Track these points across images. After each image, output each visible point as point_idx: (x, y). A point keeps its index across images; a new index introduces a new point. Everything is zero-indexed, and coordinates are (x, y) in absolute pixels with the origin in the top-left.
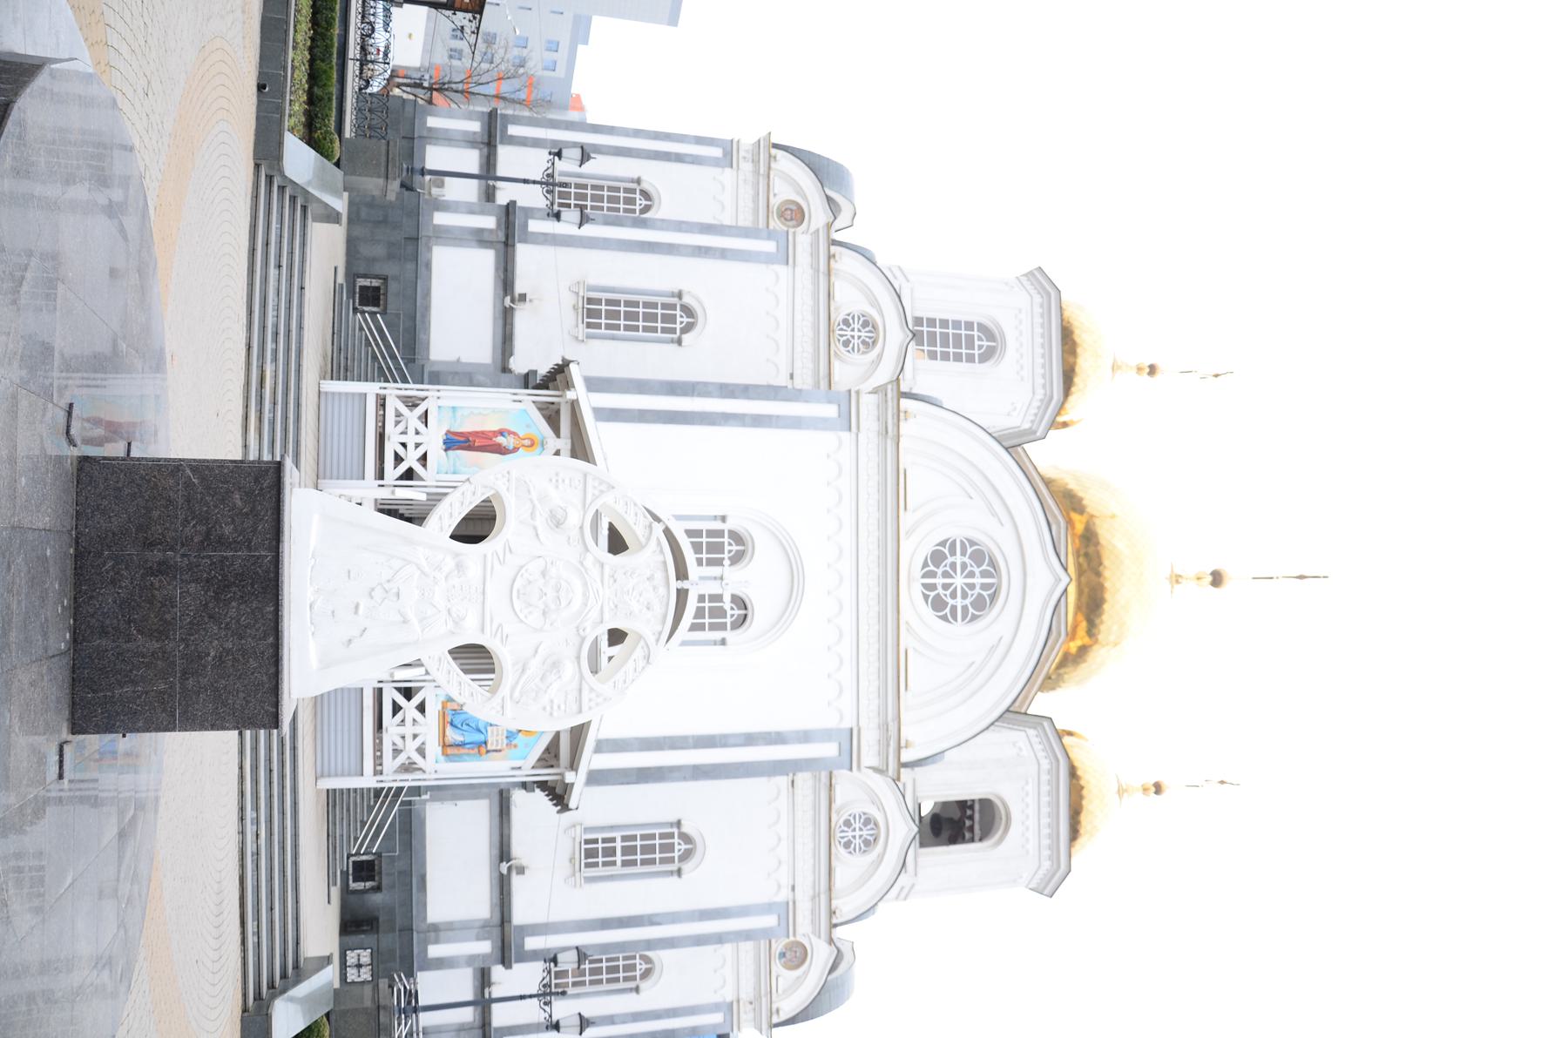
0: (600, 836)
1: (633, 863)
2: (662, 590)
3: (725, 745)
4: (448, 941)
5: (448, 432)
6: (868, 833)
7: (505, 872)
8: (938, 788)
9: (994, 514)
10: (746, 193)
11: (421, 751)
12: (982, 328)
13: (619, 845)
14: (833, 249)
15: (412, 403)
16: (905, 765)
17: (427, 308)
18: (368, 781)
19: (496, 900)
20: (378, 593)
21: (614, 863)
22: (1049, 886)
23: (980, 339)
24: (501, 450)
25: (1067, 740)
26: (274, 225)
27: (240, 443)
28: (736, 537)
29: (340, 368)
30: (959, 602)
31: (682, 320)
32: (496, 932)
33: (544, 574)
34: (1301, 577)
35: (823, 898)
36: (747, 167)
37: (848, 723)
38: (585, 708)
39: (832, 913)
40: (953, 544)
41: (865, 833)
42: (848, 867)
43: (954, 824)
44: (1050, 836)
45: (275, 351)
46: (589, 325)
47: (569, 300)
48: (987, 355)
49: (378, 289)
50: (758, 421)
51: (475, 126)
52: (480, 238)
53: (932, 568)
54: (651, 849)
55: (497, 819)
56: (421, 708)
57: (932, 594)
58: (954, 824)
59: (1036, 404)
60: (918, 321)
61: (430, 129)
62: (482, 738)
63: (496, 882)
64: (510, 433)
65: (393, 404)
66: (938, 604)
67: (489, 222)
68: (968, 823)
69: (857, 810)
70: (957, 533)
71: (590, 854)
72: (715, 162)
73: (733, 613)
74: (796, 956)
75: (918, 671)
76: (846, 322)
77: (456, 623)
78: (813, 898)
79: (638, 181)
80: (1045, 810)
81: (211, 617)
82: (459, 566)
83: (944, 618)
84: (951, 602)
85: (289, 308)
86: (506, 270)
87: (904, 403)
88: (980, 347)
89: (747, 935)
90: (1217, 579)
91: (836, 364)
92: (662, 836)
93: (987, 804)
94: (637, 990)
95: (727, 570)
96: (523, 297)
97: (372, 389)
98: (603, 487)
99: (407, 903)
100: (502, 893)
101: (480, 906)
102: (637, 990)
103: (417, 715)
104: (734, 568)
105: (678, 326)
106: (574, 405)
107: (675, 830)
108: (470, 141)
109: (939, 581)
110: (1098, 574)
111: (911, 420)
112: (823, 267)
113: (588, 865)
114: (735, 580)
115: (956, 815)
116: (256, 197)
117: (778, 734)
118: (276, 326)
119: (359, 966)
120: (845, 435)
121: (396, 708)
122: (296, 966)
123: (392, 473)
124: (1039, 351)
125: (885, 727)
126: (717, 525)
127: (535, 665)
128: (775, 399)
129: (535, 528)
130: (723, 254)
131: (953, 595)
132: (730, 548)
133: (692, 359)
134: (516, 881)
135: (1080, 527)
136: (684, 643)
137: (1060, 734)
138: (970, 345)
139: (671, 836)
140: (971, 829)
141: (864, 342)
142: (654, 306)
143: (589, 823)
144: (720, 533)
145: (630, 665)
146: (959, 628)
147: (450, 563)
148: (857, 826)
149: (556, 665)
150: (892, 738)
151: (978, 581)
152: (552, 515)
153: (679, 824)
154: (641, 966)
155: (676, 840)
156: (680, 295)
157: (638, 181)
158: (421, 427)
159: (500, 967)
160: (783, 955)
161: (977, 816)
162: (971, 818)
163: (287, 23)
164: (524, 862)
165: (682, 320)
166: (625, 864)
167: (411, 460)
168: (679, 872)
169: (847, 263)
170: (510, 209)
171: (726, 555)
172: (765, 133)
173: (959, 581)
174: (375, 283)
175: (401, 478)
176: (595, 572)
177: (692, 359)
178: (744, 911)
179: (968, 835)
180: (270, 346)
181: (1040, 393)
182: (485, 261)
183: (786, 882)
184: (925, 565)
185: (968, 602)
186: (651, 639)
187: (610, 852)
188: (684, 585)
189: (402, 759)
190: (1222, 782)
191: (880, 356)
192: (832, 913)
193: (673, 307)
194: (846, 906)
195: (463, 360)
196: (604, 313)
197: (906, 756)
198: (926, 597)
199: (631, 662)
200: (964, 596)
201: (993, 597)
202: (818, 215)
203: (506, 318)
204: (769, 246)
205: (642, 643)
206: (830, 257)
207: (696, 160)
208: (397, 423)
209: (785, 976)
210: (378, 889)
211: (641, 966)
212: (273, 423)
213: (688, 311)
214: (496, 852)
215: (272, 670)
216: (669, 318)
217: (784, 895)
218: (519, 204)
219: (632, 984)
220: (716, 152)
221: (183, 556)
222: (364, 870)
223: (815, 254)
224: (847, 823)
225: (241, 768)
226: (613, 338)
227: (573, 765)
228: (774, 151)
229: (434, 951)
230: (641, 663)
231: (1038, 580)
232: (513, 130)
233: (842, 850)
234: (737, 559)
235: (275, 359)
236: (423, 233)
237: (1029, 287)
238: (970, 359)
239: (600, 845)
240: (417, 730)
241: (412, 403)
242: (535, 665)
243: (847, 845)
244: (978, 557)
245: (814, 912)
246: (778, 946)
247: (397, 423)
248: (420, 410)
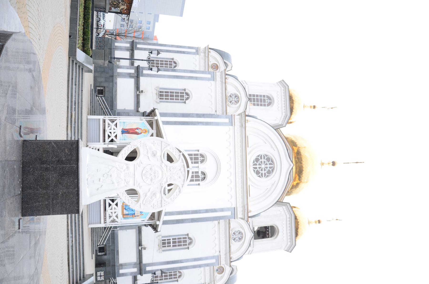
0: (166, 239)
1: (176, 246)
2: (183, 173)
3: (200, 213)
4: (125, 268)
5: (123, 129)
6: (240, 236)
7: (140, 249)
8: (259, 223)
9: (272, 147)
10: (202, 61)
11: (117, 217)
12: (267, 97)
13: (171, 241)
14: (227, 76)
15: (112, 121)
16: (250, 217)
17: (116, 95)
18: (102, 225)
19: (138, 257)
20: (106, 175)
21: (170, 246)
22: (290, 249)
23: (267, 100)
24: (137, 133)
25: (294, 209)
26: (74, 74)
27: (66, 133)
28: (202, 156)
29: (93, 112)
30: (263, 172)
31: (186, 96)
32: (138, 266)
33: (151, 169)
34: (357, 163)
35: (228, 254)
36: (202, 54)
37: (234, 206)
38: (163, 206)
39: (230, 258)
40: (261, 156)
41: (239, 236)
42: (235, 245)
43: (263, 233)
44: (290, 236)
45: (75, 108)
46: (160, 99)
47: (155, 92)
48: (269, 104)
49: (102, 90)
50: (207, 124)
51: (128, 45)
52: (130, 76)
53: (256, 163)
54: (180, 242)
55: (138, 235)
56: (117, 205)
57: (256, 170)
58: (263, 233)
59: (283, 117)
60: (250, 95)
61: (116, 46)
62: (133, 212)
63: (138, 252)
64: (140, 129)
65: (107, 122)
66: (258, 173)
67: (132, 71)
68: (267, 233)
69: (237, 230)
70: (262, 153)
71: (164, 243)
72: (194, 53)
73: (201, 176)
74: (221, 270)
75: (253, 192)
76: (230, 96)
77: (127, 183)
78: (225, 254)
79: (173, 59)
80: (288, 228)
81: (60, 183)
82: (128, 168)
83: (259, 176)
84: (261, 172)
85: (79, 96)
86: (137, 84)
87: (247, 118)
88: (267, 102)
89: (207, 265)
90: (334, 164)
91: (228, 108)
92: (183, 238)
93: (272, 227)
94: (177, 281)
95: (200, 164)
96: (142, 91)
97: (101, 117)
98: (167, 145)
99: (114, 258)
100: (140, 255)
101: (134, 259)
102: (177, 281)
103: (116, 207)
104: (202, 164)
105: (185, 98)
106: (157, 121)
107: (187, 237)
108: (127, 49)
109: (258, 166)
110: (301, 163)
111: (249, 122)
112: (224, 81)
113: (163, 247)
114: (202, 167)
115: (264, 230)
116: (69, 66)
117: (215, 209)
118: (75, 101)
119: (101, 276)
120: (231, 127)
121: (110, 205)
122: (84, 277)
123: (107, 140)
124: (283, 103)
125: (244, 207)
126: (197, 152)
127: (149, 194)
128: (212, 118)
129: (148, 157)
130: (196, 78)
131: (262, 170)
132: (200, 159)
133: (188, 107)
134: (144, 252)
135: (296, 151)
136: (189, 185)
137: (292, 208)
138: (264, 101)
139: (186, 238)
140: (268, 234)
141: (235, 101)
142: (178, 93)
143: (163, 235)
144: (197, 155)
145: (175, 193)
146: (263, 179)
147: (125, 167)
148: (237, 234)
149: (155, 194)
150: (246, 209)
151: (268, 166)
152: (153, 153)
153: (188, 235)
154: (178, 274)
155: (187, 239)
156: (185, 90)
157: (173, 59)
158: (115, 128)
159: (140, 275)
160: (217, 270)
161: (270, 231)
162: (268, 231)
163: (77, 19)
164: (146, 246)
166: (173, 246)
167: (113, 137)
168: (188, 248)
169: (230, 80)
170: (138, 67)
171: (199, 161)
172: (207, 45)
173: (263, 166)
174: (102, 88)
175: (110, 142)
176: (165, 168)
177: (188, 107)
178: (206, 258)
179: (267, 236)
180: (73, 107)
181: (284, 114)
182: (132, 81)
183: (218, 250)
184: (254, 162)
185: (266, 172)
186: (181, 186)
187: (169, 243)
188: (189, 169)
189: (112, 219)
190: (337, 220)
191: (240, 105)
192: (230, 258)
193: (183, 93)
194: (234, 256)
195: (126, 109)
196: (164, 95)
197: (250, 215)
198: (254, 171)
199: (175, 192)
200: (265, 170)
201: (273, 170)
202: (222, 67)
203: (137, 97)
204: (209, 76)
205: (178, 188)
206: (226, 78)
207: (188, 53)
208: (109, 127)
209: (218, 276)
210: (106, 254)
211: (178, 274)
212: (75, 127)
213: (187, 94)
214: (138, 244)
215: (77, 198)
216: (182, 96)
217: (217, 254)
218: (141, 66)
219: (176, 279)
220: (194, 51)
221: (52, 167)
222: (102, 249)
223: (221, 78)
224: (234, 233)
225: (68, 222)
226: (167, 102)
227: (159, 219)
228: (209, 50)
229: (121, 271)
230: (178, 193)
231: (285, 165)
232: (138, 46)
233: (233, 241)
234: (202, 161)
235: (75, 110)
236: (114, 74)
237: (280, 85)
238: (265, 105)
239: (166, 241)
240: (116, 211)
241: (112, 121)
242: (149, 194)
243: (234, 239)
244: (268, 159)
245: (226, 258)
246: (216, 268)
247: (109, 127)
248: (115, 123)
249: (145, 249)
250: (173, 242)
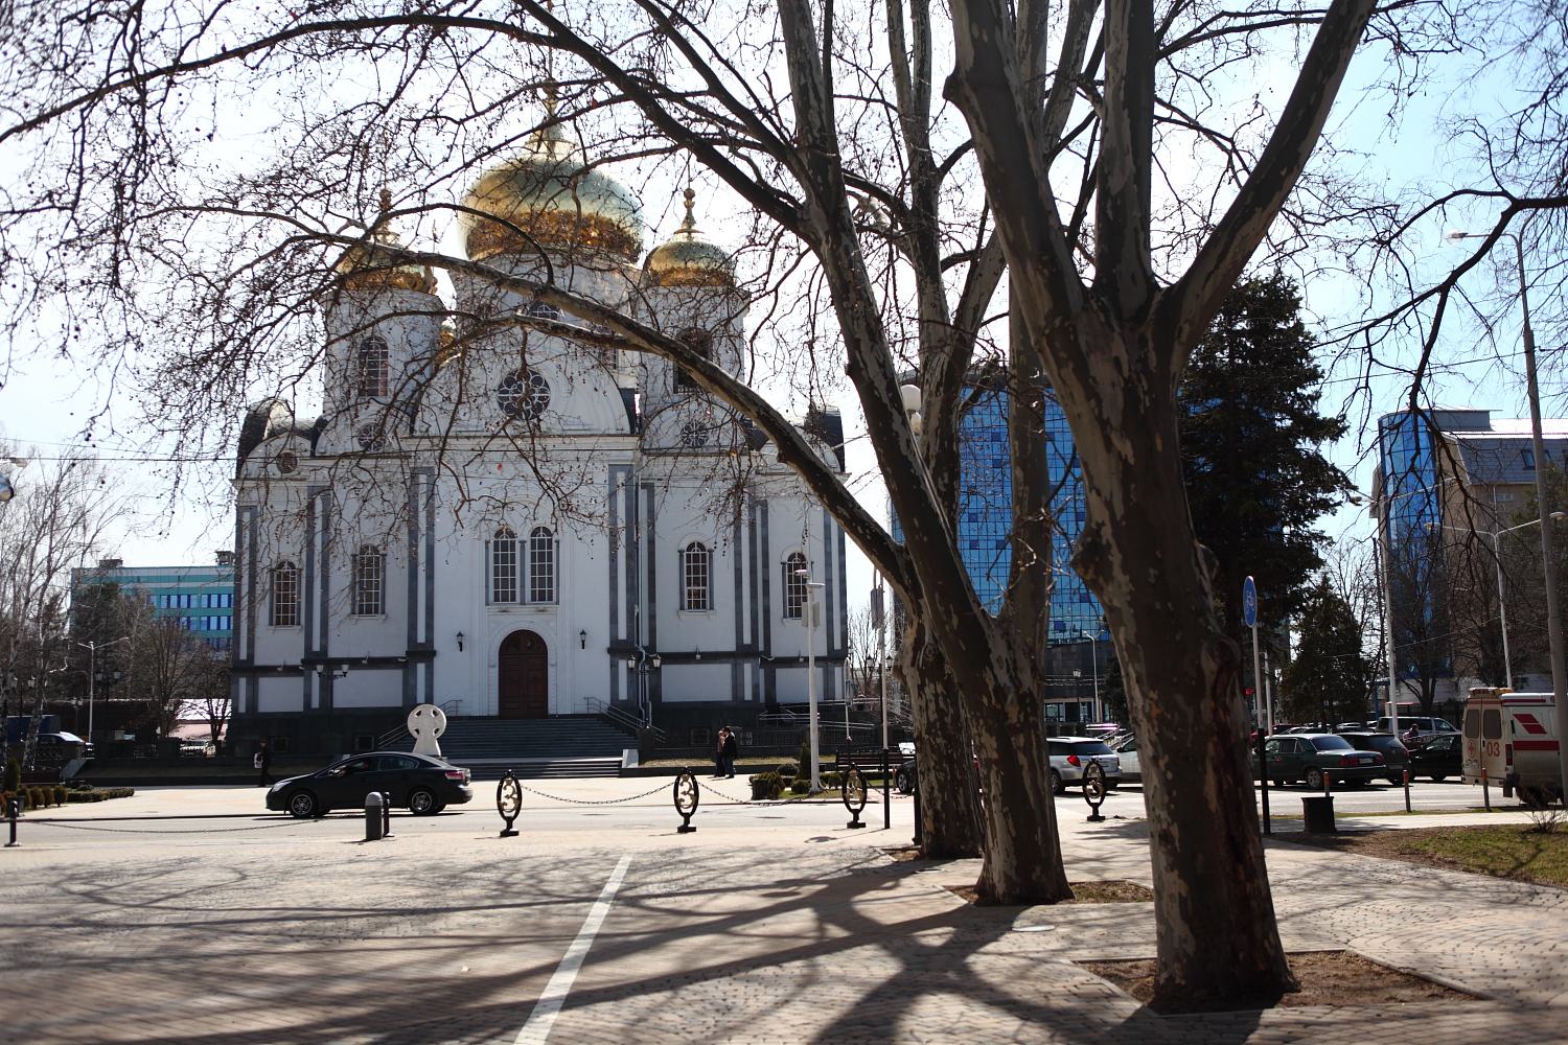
1: (704, 579)
114: (524, 533)
146: (553, 395)
187: (697, 594)
196: (368, 601)
232: (243, 656)
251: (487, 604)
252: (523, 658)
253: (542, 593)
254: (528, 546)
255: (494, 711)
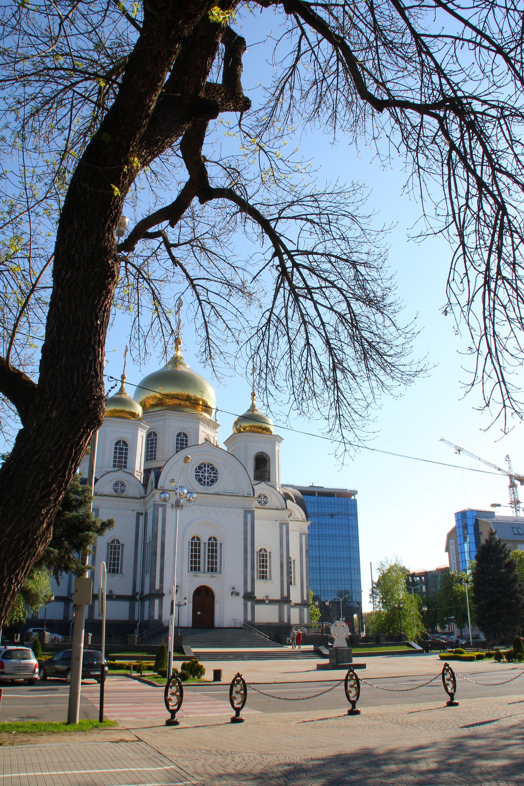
1: (266, 566)
13: (261, 569)
28: (193, 539)
30: (212, 475)
46: (117, 572)
60: (114, 466)
66: (213, 482)
70: (194, 473)
101: (275, 608)
114: (204, 539)
138: (122, 449)
165: (115, 543)
166: (266, 568)
183: (275, 522)
191: (127, 481)
193: (111, 546)
197: (252, 495)
198: (211, 485)
213: (113, 541)
229: (286, 621)
234: (198, 539)
238: (126, 450)
249: (267, 597)
250: (263, 568)
251: (188, 572)
252: (204, 598)
253: (212, 568)
254: (207, 545)
255: (190, 625)
